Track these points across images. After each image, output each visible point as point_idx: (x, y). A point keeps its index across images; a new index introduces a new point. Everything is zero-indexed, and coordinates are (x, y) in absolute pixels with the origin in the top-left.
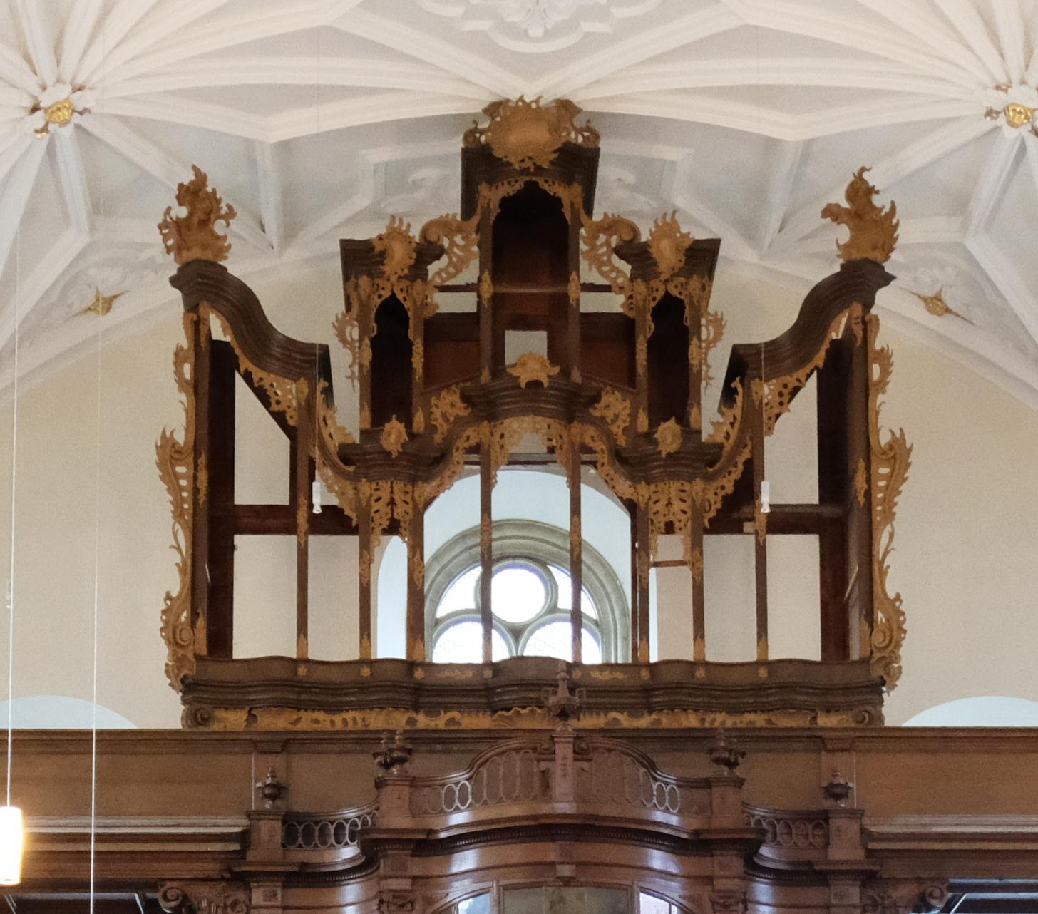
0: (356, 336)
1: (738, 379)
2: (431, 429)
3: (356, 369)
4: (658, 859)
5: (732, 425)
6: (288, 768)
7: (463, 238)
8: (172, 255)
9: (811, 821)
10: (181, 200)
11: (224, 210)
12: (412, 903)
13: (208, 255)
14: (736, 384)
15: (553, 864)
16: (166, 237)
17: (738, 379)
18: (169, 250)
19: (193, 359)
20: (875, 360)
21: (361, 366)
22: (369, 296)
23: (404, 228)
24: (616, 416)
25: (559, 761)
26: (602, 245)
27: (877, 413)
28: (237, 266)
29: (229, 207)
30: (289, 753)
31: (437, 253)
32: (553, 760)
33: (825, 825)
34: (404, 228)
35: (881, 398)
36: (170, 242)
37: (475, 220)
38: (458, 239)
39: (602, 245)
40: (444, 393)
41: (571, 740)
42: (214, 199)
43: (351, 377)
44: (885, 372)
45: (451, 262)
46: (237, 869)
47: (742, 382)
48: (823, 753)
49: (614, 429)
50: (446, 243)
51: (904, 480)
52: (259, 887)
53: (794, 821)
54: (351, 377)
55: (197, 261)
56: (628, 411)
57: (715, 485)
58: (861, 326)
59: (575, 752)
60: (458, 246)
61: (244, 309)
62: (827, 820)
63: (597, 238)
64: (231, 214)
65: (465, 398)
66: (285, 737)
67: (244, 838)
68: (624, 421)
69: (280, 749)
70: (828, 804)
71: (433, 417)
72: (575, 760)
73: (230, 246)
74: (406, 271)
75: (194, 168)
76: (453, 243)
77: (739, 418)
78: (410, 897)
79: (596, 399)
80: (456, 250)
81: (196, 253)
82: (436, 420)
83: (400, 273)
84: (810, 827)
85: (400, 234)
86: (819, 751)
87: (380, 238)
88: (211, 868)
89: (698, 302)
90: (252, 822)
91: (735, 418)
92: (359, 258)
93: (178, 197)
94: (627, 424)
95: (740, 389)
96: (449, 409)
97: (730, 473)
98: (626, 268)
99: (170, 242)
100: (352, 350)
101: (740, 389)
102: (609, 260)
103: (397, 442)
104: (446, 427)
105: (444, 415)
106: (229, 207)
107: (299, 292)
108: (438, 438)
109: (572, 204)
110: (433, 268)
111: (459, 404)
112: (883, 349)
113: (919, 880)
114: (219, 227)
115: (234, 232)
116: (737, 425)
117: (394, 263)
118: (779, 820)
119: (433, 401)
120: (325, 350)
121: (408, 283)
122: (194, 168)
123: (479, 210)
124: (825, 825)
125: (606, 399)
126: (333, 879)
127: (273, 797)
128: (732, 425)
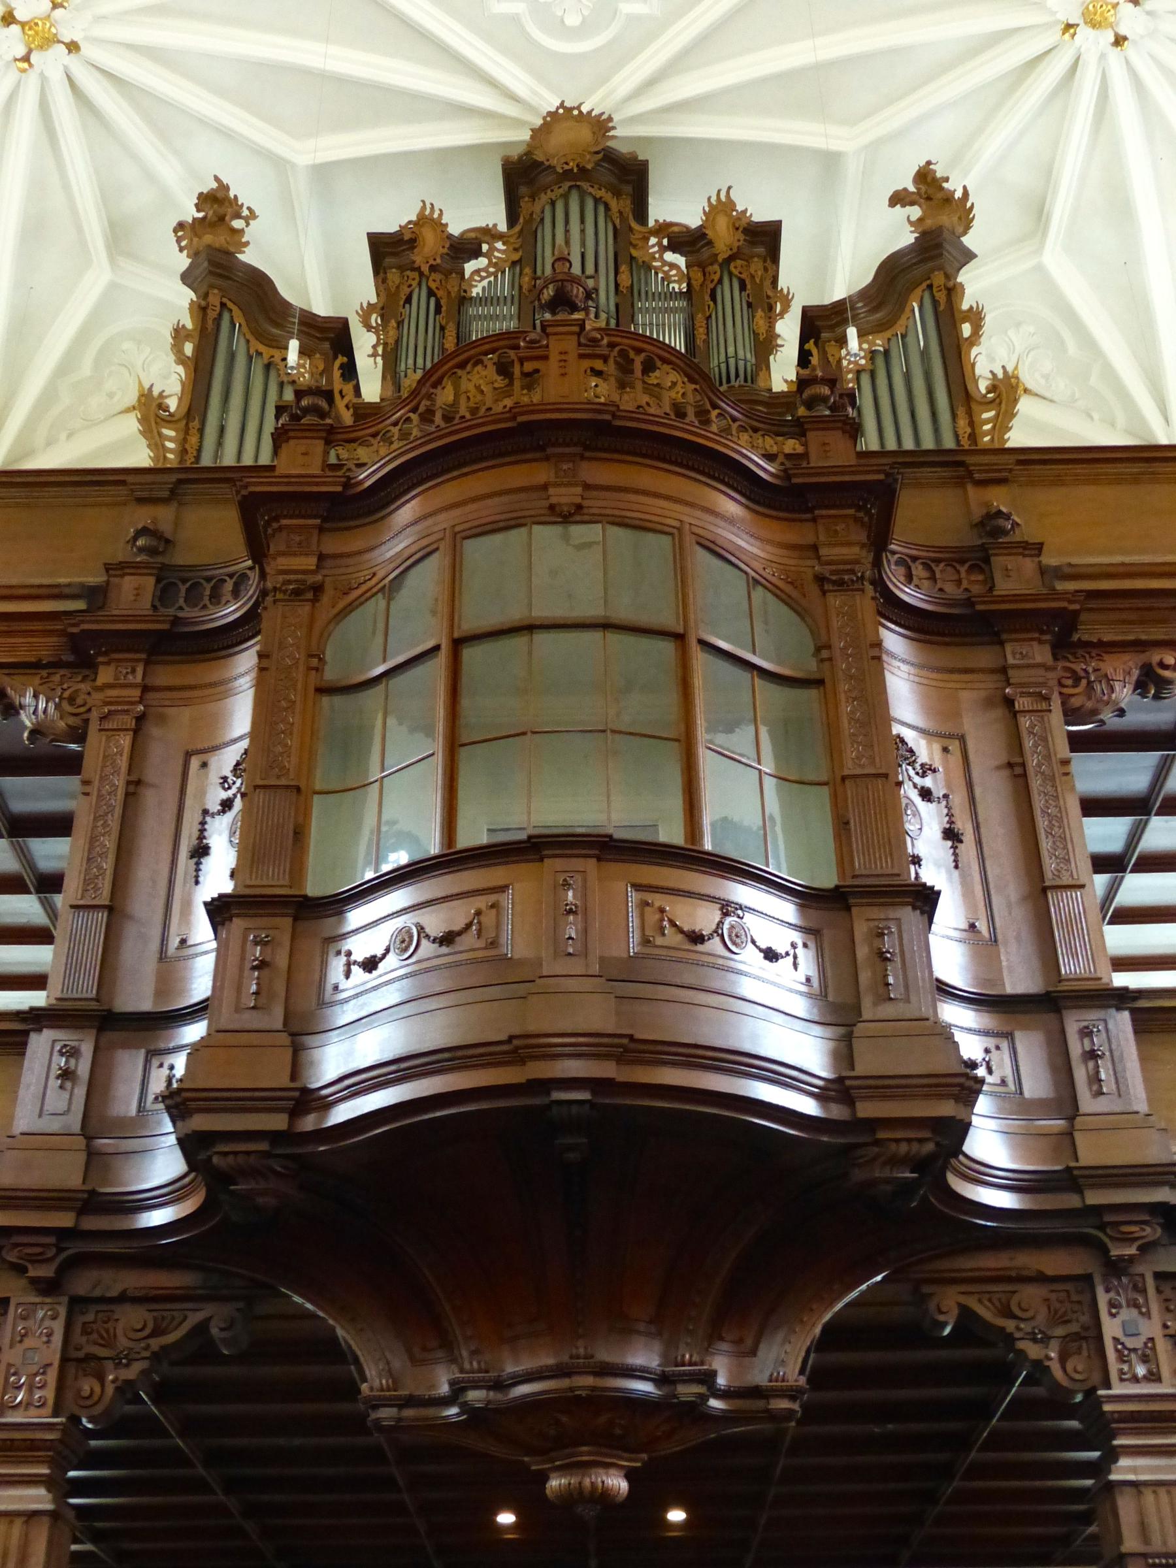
1: (812, 341)
3: (380, 350)
4: (728, 514)
6: (177, 524)
7: (504, 244)
8: (185, 252)
9: (962, 562)
11: (245, 213)
12: (318, 589)
14: (810, 345)
15: (545, 487)
16: (179, 241)
17: (812, 341)
18: (181, 250)
19: (196, 340)
20: (964, 321)
21: (385, 345)
22: (398, 287)
23: (436, 216)
25: (554, 357)
26: (653, 246)
27: (973, 365)
29: (249, 208)
30: (180, 504)
31: (477, 253)
32: (545, 358)
33: (983, 566)
34: (436, 216)
35: (974, 351)
36: (183, 244)
37: (517, 228)
39: (653, 246)
41: (576, 329)
43: (374, 355)
44: (977, 328)
45: (490, 264)
46: (75, 630)
47: (816, 344)
48: (970, 488)
50: (485, 247)
51: (1013, 415)
52: (108, 663)
53: (938, 561)
54: (374, 355)
55: (209, 246)
58: (945, 292)
59: (580, 344)
60: (499, 251)
62: (987, 560)
63: (648, 239)
64: (253, 215)
67: (96, 595)
69: (166, 494)
73: (247, 244)
78: (311, 579)
83: (432, 262)
84: (963, 570)
85: (433, 220)
88: (45, 647)
89: (761, 280)
90: (112, 579)
92: (387, 250)
93: (196, 205)
95: (815, 351)
98: (680, 260)
99: (183, 244)
100: (377, 333)
101: (815, 351)
102: (661, 257)
106: (249, 208)
109: (621, 213)
110: (470, 267)
112: (971, 307)
113: (1139, 646)
118: (914, 559)
120: (344, 324)
123: (521, 220)
124: (983, 566)
126: (222, 642)
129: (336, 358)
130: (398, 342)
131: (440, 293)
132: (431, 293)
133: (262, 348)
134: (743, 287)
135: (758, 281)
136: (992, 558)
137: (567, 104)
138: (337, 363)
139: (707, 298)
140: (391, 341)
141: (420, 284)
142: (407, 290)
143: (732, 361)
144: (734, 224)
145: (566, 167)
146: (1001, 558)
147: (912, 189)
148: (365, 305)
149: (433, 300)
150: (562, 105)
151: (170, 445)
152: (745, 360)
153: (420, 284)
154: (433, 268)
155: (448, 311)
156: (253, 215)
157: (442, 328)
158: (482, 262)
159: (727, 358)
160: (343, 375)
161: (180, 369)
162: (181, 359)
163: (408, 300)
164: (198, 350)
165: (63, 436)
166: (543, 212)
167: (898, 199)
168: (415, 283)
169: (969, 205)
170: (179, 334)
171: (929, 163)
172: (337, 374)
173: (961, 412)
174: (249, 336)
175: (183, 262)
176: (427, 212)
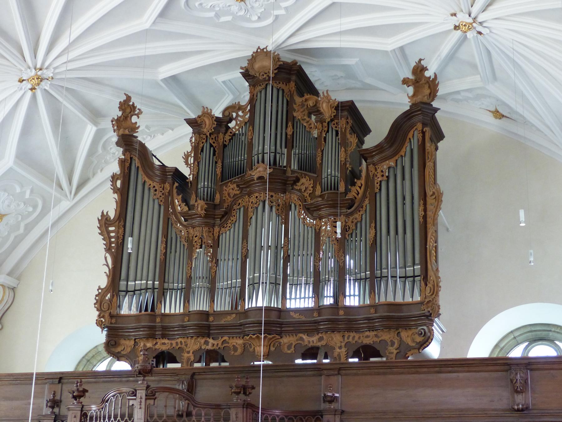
0: (192, 162)
2: (222, 201)
5: (360, 188)
7: (243, 112)
9: (313, 416)
10: (120, 108)
13: (127, 132)
16: (113, 127)
24: (306, 188)
28: (141, 136)
34: (209, 111)
38: (240, 113)
40: (229, 184)
42: (133, 107)
49: (305, 194)
50: (234, 115)
56: (312, 185)
57: (351, 218)
60: (240, 116)
61: (144, 154)
65: (238, 186)
66: (59, 376)
68: (310, 190)
70: (324, 406)
71: (224, 196)
72: (146, 399)
73: (139, 127)
74: (213, 130)
75: (125, 94)
76: (238, 115)
77: (363, 184)
79: (297, 180)
80: (239, 118)
81: (121, 132)
82: (225, 197)
83: (210, 132)
85: (208, 114)
86: (321, 375)
87: (199, 117)
91: (362, 185)
94: (311, 192)
96: (231, 191)
97: (359, 211)
103: (202, 210)
104: (230, 199)
105: (229, 194)
107: (170, 145)
108: (226, 205)
111: (236, 188)
114: (134, 119)
115: (141, 122)
116: (362, 188)
117: (207, 126)
118: (296, 417)
119: (224, 188)
121: (216, 135)
122: (125, 94)
125: (303, 180)
127: (52, 407)
128: (360, 188)
129: (174, 184)
130: (198, 173)
131: (214, 145)
132: (211, 146)
133: (147, 180)
134: (337, 134)
135: (343, 130)
136: (324, 416)
137: (262, 48)
138: (175, 186)
139: (323, 140)
140: (195, 173)
141: (206, 141)
142: (202, 145)
143: (329, 177)
144: (331, 106)
145: (263, 77)
146: (327, 416)
147: (411, 77)
148: (186, 153)
149: (212, 148)
150: (259, 48)
151: (113, 234)
152: (335, 176)
153: (206, 141)
154: (210, 134)
155: (218, 154)
156: (141, 112)
157: (216, 163)
158: (234, 123)
159: (328, 175)
160: (177, 192)
161: (116, 196)
162: (115, 190)
163: (202, 151)
164: (123, 184)
165: (99, 171)
166: (257, 96)
167: (405, 82)
168: (204, 141)
169: (437, 82)
170: (114, 178)
171: (420, 60)
172: (175, 191)
173: (422, 202)
174: (143, 173)
175: (115, 139)
176: (206, 110)
